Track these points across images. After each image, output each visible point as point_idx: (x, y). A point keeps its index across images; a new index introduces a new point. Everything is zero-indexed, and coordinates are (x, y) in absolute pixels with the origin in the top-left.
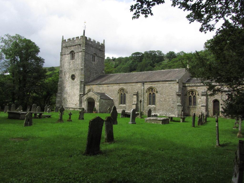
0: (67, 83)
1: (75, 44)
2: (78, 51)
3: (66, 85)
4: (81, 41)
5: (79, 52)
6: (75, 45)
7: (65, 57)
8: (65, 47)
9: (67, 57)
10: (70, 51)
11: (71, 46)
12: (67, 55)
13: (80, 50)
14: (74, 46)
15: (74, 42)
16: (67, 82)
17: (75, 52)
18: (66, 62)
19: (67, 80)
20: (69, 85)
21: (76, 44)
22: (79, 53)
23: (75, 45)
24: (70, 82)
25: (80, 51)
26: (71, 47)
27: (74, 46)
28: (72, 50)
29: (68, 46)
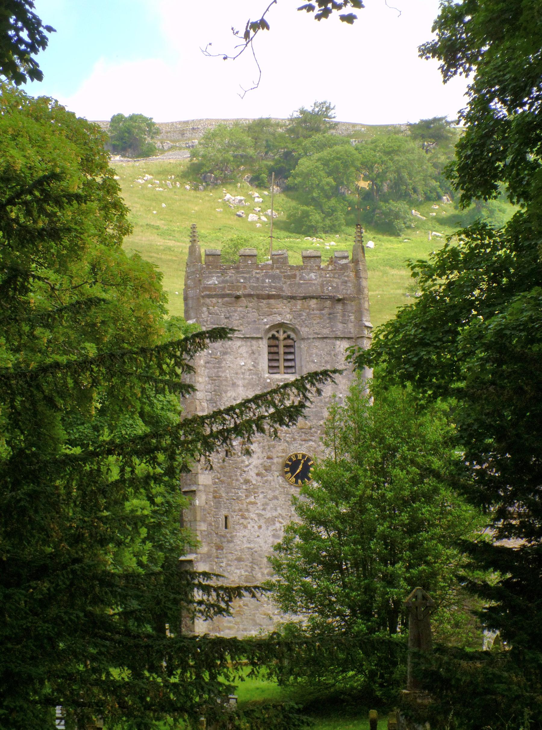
0: (252, 499)
1: (301, 292)
2: (326, 332)
3: (248, 510)
4: (346, 282)
5: (337, 338)
6: (305, 298)
7: (225, 353)
8: (223, 296)
9: (244, 350)
10: (268, 321)
11: (269, 297)
12: (239, 343)
13: (340, 326)
14: (292, 298)
15: (294, 276)
16: (248, 493)
17: (304, 331)
18: (240, 383)
19: (247, 482)
20: (268, 515)
21: (311, 290)
22: (334, 345)
23: (305, 298)
24: (276, 498)
25: (339, 334)
26: (272, 301)
27: (292, 298)
28: (279, 319)
29: (250, 296)
